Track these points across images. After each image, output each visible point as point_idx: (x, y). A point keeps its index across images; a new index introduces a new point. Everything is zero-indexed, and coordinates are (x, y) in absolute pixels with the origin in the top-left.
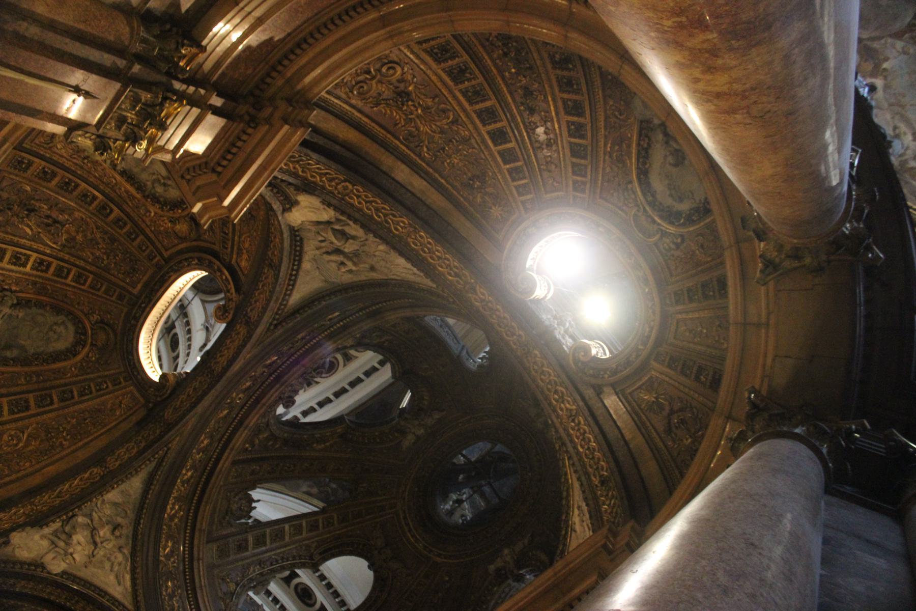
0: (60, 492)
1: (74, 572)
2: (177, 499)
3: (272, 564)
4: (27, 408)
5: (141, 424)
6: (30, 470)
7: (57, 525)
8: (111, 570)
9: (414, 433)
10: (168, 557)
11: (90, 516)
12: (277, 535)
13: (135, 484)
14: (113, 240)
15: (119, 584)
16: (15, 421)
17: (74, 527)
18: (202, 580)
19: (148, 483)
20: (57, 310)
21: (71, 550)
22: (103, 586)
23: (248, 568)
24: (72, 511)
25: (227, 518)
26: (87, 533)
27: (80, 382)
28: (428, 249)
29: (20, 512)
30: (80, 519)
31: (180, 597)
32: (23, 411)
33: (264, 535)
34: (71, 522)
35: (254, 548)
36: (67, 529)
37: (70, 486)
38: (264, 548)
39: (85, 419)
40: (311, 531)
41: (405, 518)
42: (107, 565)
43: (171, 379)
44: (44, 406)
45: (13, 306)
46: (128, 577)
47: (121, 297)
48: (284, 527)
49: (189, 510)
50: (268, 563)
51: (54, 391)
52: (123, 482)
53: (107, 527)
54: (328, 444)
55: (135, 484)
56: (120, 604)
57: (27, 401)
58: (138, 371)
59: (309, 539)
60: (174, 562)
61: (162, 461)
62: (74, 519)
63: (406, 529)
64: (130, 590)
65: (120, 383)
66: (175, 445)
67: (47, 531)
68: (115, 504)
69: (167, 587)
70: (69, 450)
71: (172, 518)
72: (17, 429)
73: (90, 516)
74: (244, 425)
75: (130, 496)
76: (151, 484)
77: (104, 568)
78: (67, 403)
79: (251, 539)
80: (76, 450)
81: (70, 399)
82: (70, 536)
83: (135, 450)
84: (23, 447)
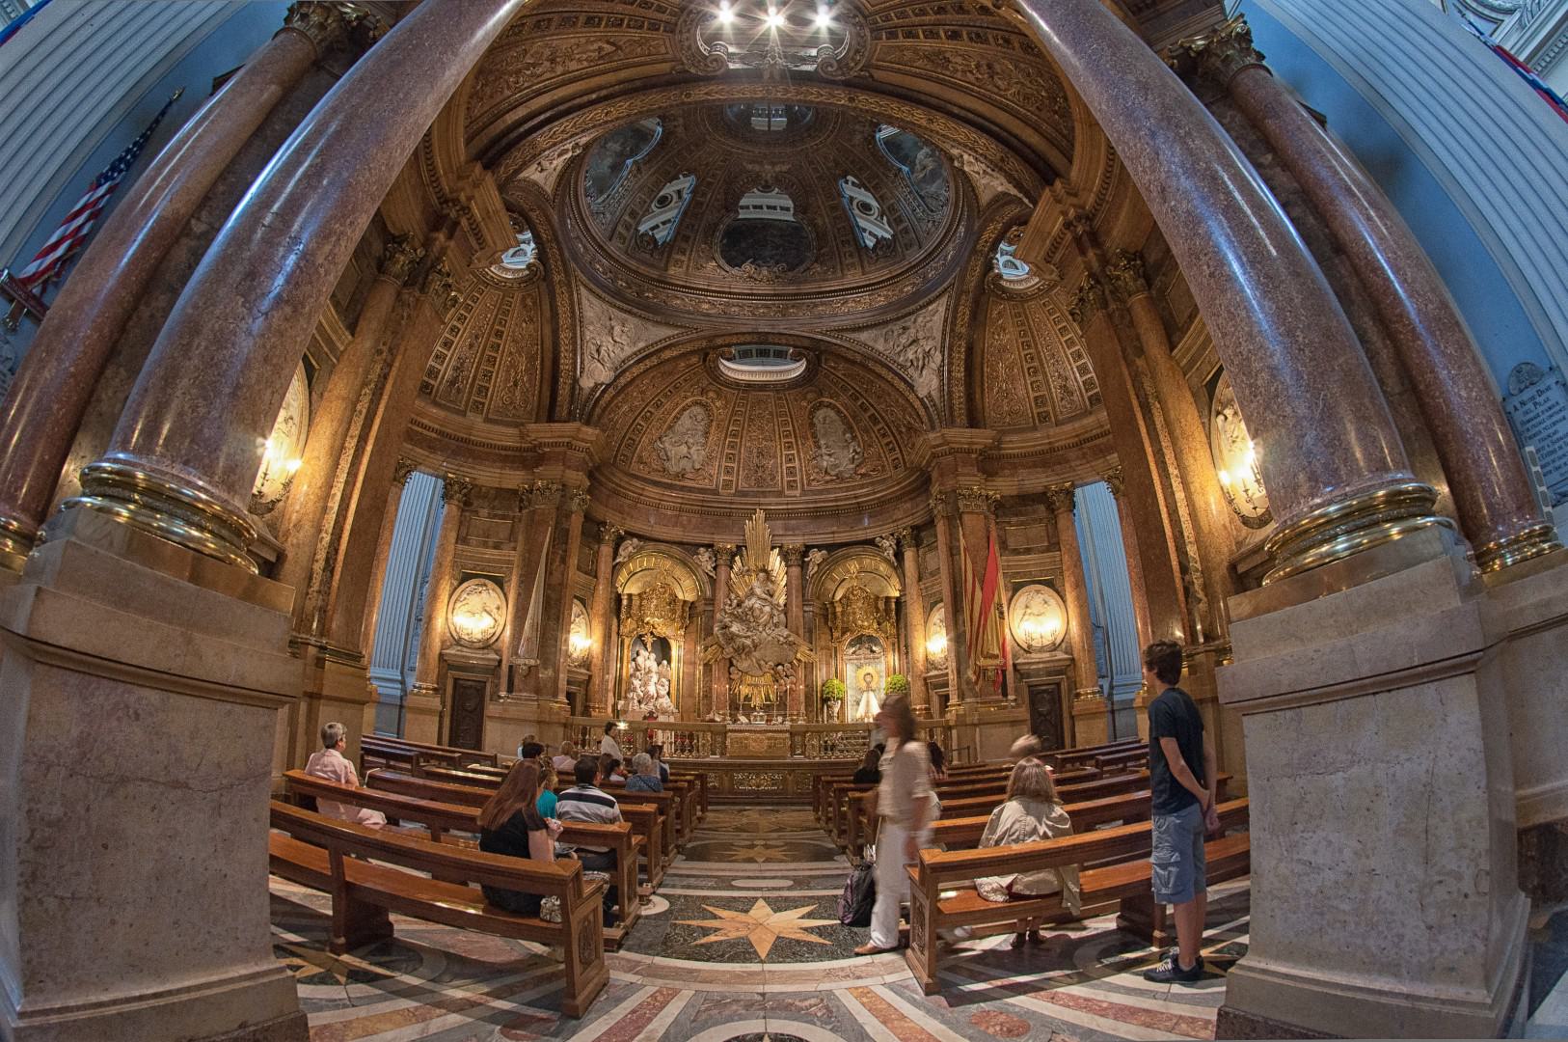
14: (751, 420)
16: (882, 418)
20: (812, 425)
29: (911, 398)
42: (929, 325)
45: (819, 448)
46: (930, 308)
47: (780, 399)
68: (886, 340)
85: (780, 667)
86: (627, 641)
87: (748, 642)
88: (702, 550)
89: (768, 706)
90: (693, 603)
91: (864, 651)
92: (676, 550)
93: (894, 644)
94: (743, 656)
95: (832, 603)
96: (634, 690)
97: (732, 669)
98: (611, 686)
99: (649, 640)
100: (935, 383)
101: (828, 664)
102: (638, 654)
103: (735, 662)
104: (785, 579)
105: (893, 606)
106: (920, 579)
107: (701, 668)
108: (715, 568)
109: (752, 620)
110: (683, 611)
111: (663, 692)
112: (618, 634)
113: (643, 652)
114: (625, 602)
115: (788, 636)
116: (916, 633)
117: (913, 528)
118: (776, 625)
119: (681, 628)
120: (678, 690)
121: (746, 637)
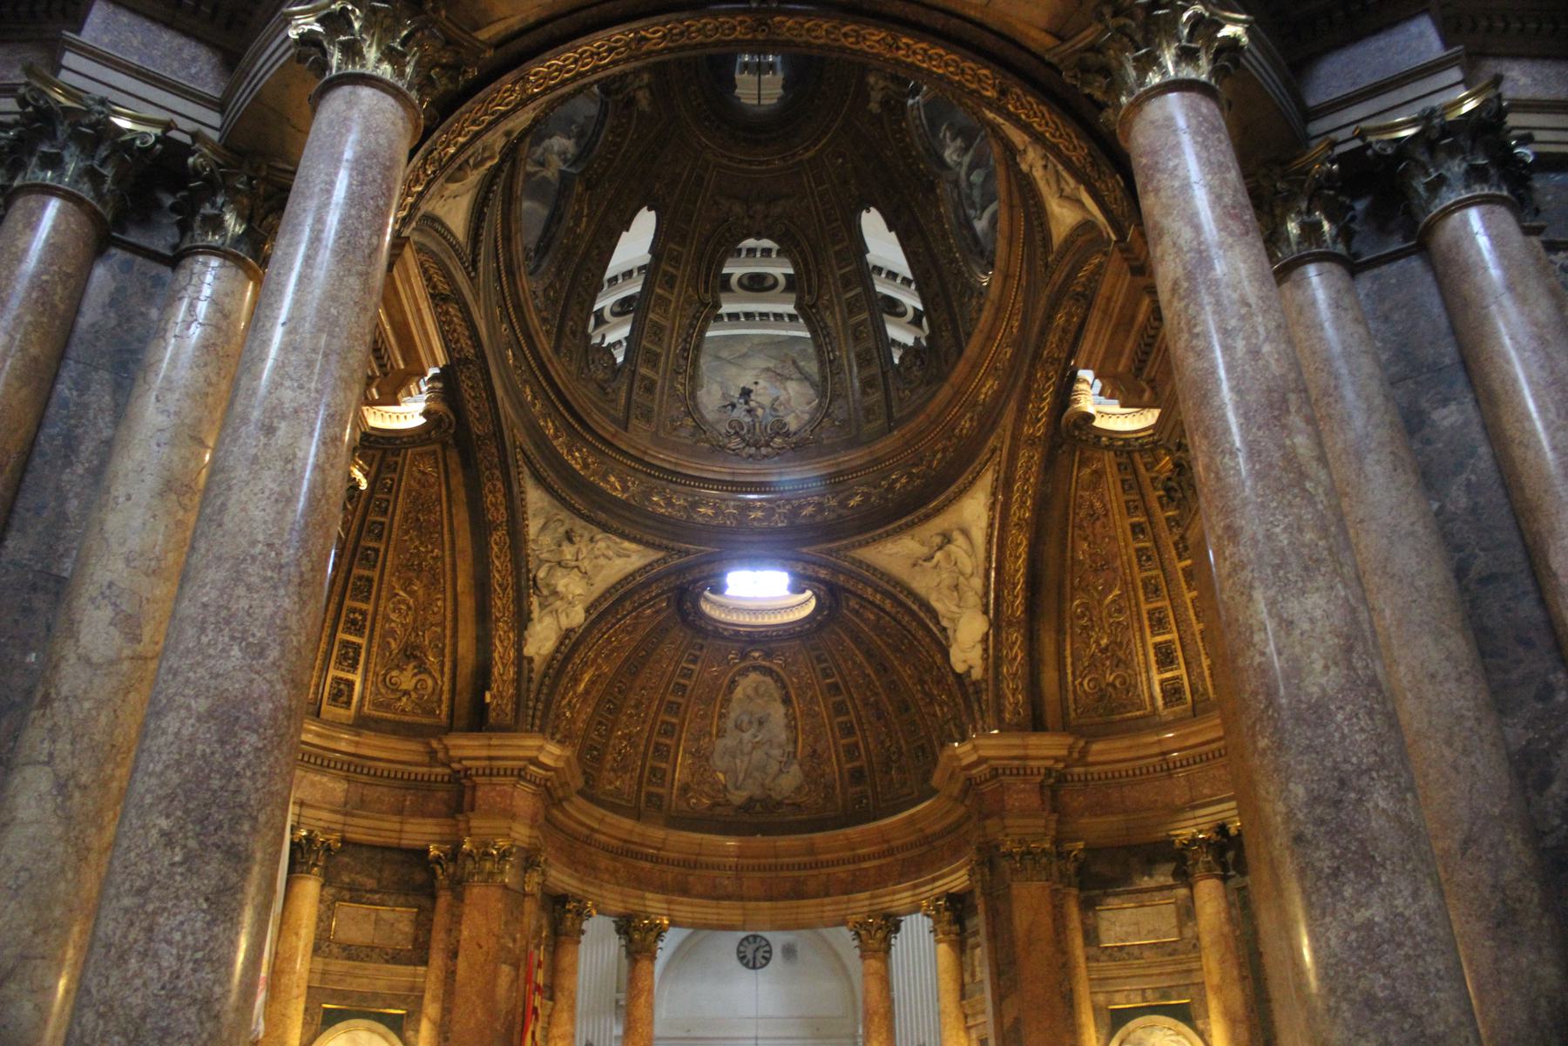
0: (500, 586)
1: (591, 599)
2: (570, 452)
3: (687, 358)
4: (370, 580)
5: (468, 463)
6: (449, 604)
7: (535, 600)
8: (610, 559)
9: (640, 88)
10: (625, 489)
11: (542, 562)
12: (655, 334)
13: (535, 497)
15: (629, 556)
17: (548, 585)
18: (664, 458)
19: (541, 481)
21: (570, 597)
22: (621, 575)
23: (676, 390)
24: (528, 580)
25: (609, 390)
26: (559, 572)
27: (366, 509)
28: (556, 70)
30: (541, 574)
31: (675, 492)
32: (371, 587)
33: (648, 351)
34: (540, 585)
35: (657, 373)
36: (545, 592)
37: (499, 571)
38: (663, 359)
39: (418, 519)
40: (672, 287)
41: (731, 159)
42: (602, 561)
43: (434, 406)
44: (376, 561)
46: (626, 544)
48: (651, 320)
49: (585, 438)
50: (682, 362)
51: (362, 543)
52: (525, 512)
53: (564, 548)
54: (586, 211)
55: (535, 497)
56: (650, 564)
57: (360, 578)
58: (397, 438)
59: (680, 295)
60: (633, 483)
61: (528, 458)
62: (539, 581)
63: (745, 166)
64: (641, 548)
65: (396, 463)
66: (521, 437)
67: (535, 615)
68: (544, 527)
69: (657, 504)
70: (447, 553)
71: (586, 466)
72: (388, 600)
73: (542, 562)
74: (533, 332)
75: (542, 508)
76: (545, 480)
77: (602, 567)
78: (386, 533)
79: (643, 371)
80: (453, 544)
81: (383, 529)
82: (555, 593)
83: (499, 485)
84: (416, 600)
100: (548, 646)
106: (316, 950)
117: (344, 841)
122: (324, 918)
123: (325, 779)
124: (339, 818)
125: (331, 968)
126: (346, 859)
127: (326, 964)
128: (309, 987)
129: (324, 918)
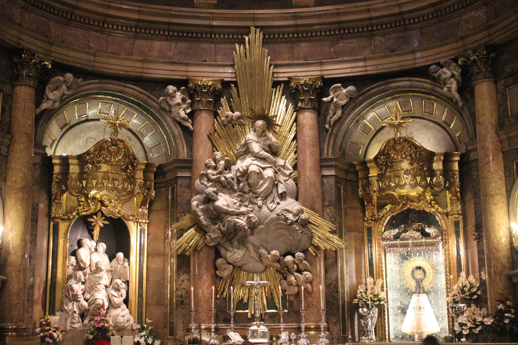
85: (289, 258)
86: (63, 227)
87: (242, 221)
88: (171, 88)
89: (272, 315)
90: (160, 167)
91: (413, 234)
92: (132, 89)
93: (457, 224)
94: (235, 243)
95: (364, 163)
96: (75, 298)
97: (219, 261)
98: (38, 294)
99: (99, 223)
101: (359, 252)
102: (80, 244)
103: (223, 251)
104: (294, 129)
105: (456, 166)
107: (174, 261)
108: (191, 115)
109: (247, 189)
110: (146, 179)
111: (118, 300)
112: (49, 217)
113: (89, 243)
114: (57, 169)
115: (301, 211)
116: (493, 208)
117: (491, 48)
118: (283, 196)
119: (143, 204)
120: (140, 295)
121: (239, 215)
122: (502, 102)
123: (473, 13)
124: (485, 33)
125: (512, 134)
126: (506, 56)
127: (507, 134)
128: (503, 153)
129: (502, 102)
